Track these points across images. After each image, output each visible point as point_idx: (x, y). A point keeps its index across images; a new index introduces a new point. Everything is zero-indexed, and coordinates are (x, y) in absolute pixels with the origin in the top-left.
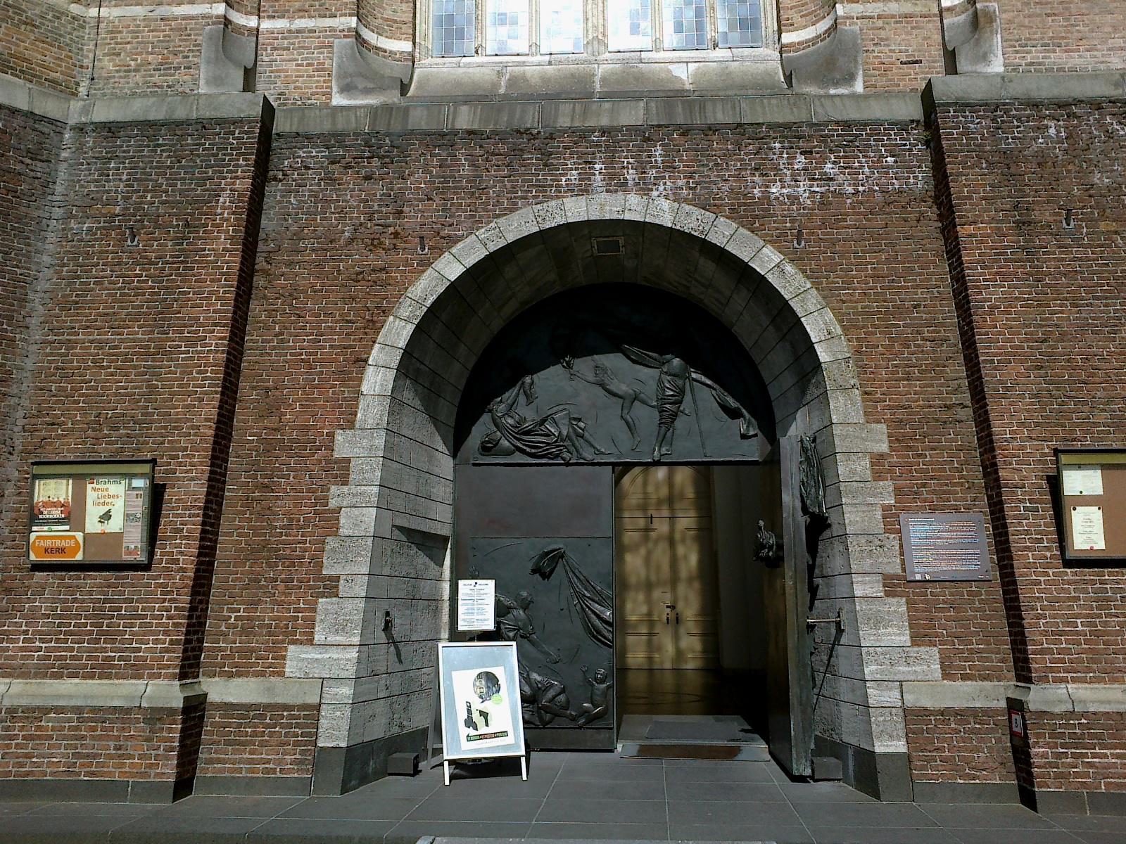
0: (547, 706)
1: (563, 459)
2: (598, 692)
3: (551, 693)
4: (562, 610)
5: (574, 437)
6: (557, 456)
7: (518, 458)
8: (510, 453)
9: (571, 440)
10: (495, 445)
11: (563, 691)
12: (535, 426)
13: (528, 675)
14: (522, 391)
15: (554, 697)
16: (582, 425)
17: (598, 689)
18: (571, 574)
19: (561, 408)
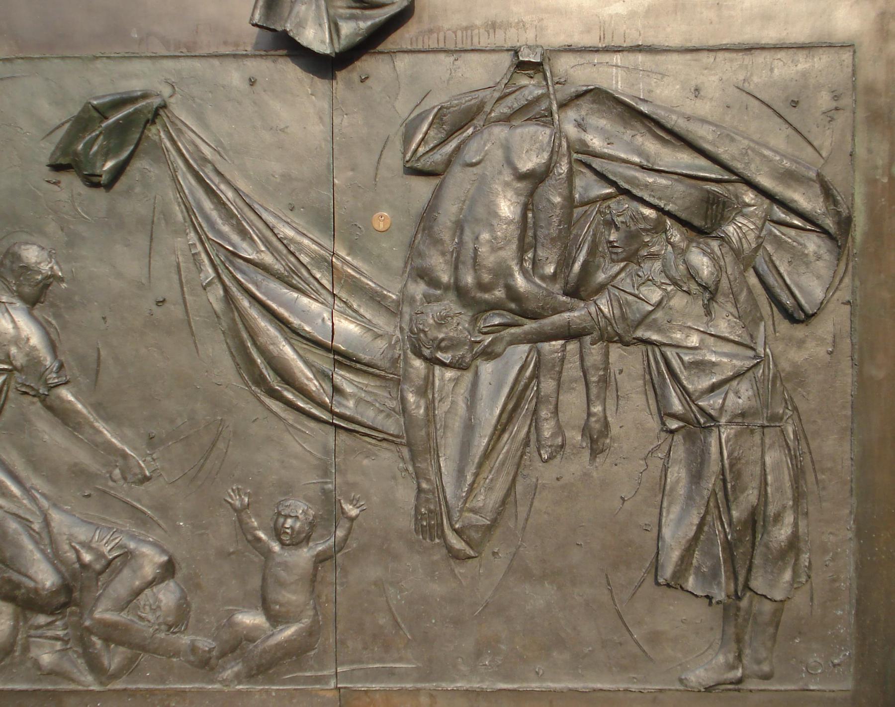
0: (114, 625)
2: (283, 574)
3: (123, 584)
4: (160, 303)
11: (169, 570)
13: (47, 522)
15: (138, 592)
17: (285, 566)
18: (187, 181)
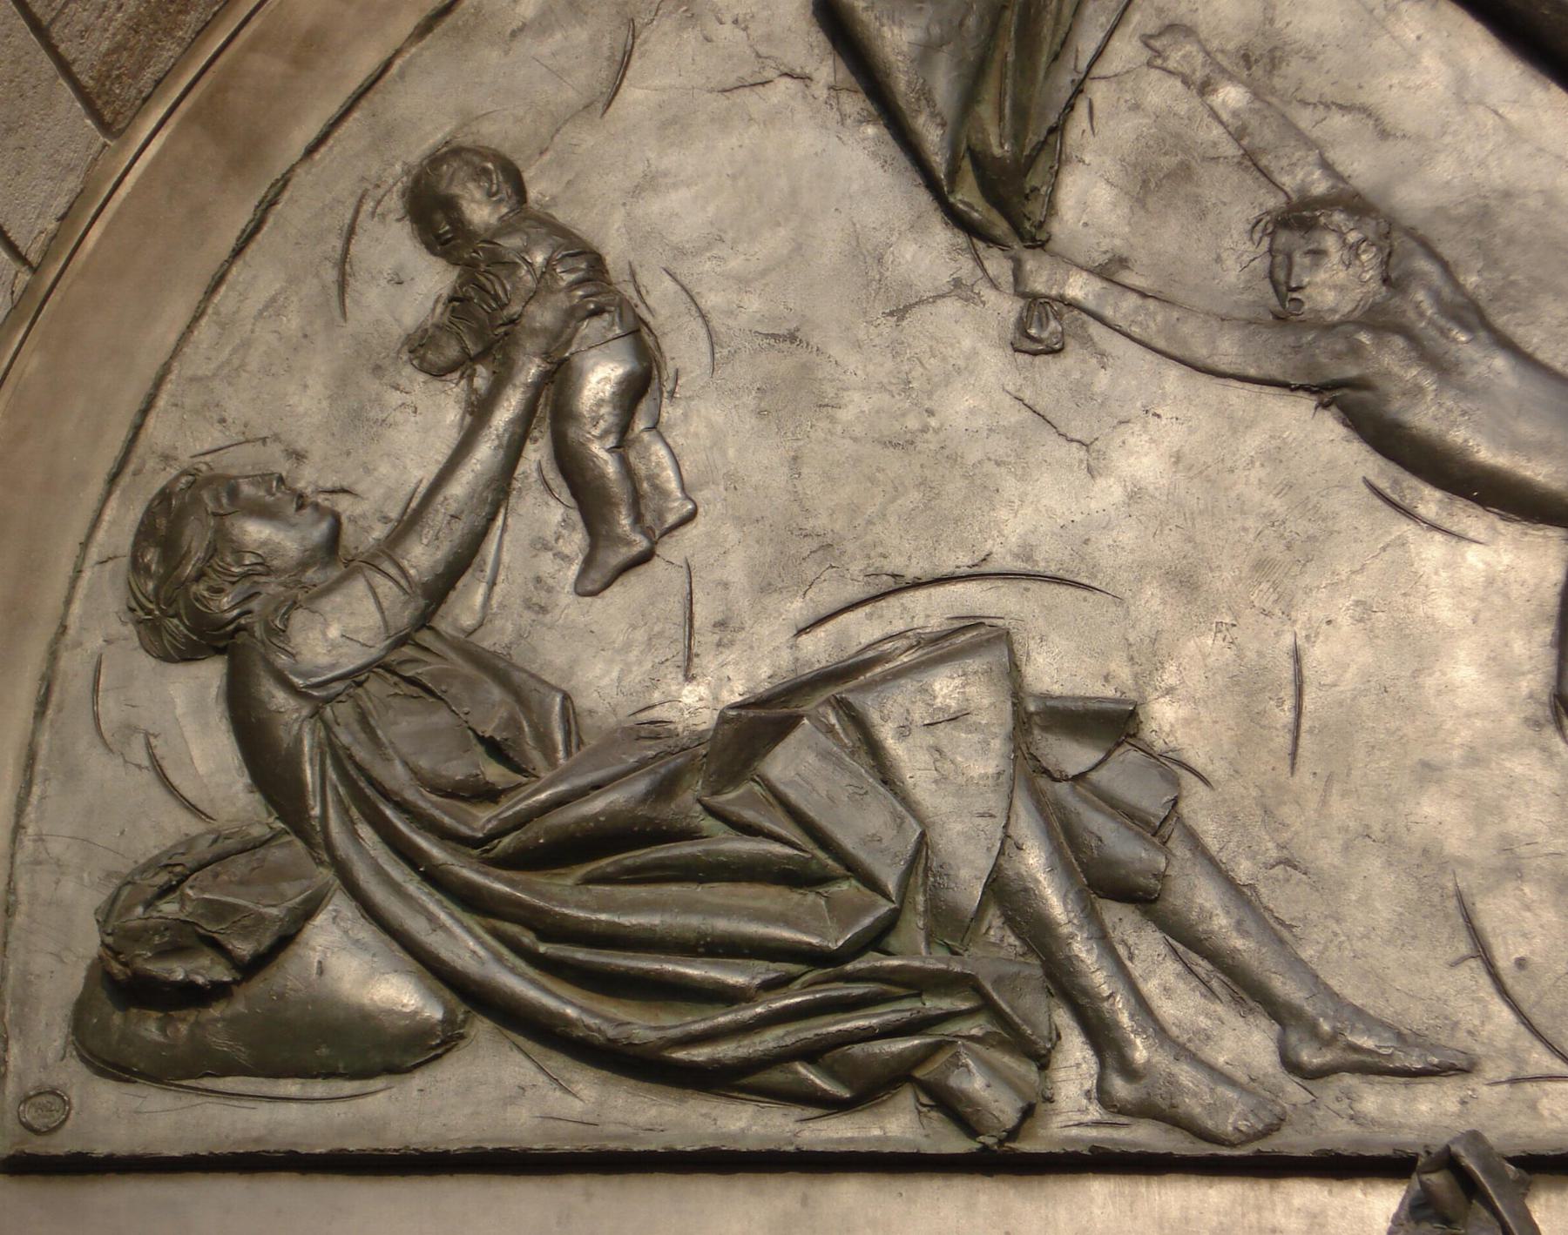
1: (950, 1106)
5: (1056, 904)
6: (870, 1090)
7: (493, 1089)
8: (394, 1051)
9: (1037, 934)
10: (252, 968)
12: (666, 789)
14: (537, 454)
16: (1123, 776)
19: (929, 610)
